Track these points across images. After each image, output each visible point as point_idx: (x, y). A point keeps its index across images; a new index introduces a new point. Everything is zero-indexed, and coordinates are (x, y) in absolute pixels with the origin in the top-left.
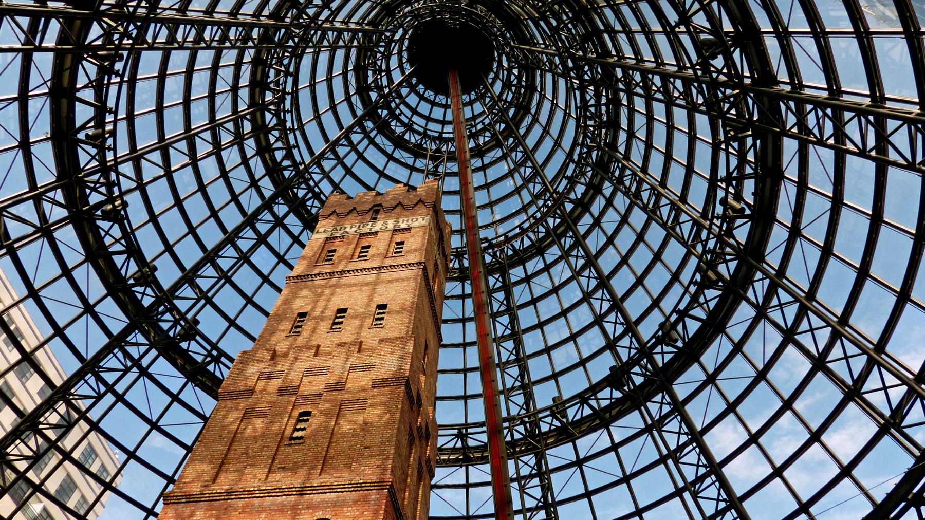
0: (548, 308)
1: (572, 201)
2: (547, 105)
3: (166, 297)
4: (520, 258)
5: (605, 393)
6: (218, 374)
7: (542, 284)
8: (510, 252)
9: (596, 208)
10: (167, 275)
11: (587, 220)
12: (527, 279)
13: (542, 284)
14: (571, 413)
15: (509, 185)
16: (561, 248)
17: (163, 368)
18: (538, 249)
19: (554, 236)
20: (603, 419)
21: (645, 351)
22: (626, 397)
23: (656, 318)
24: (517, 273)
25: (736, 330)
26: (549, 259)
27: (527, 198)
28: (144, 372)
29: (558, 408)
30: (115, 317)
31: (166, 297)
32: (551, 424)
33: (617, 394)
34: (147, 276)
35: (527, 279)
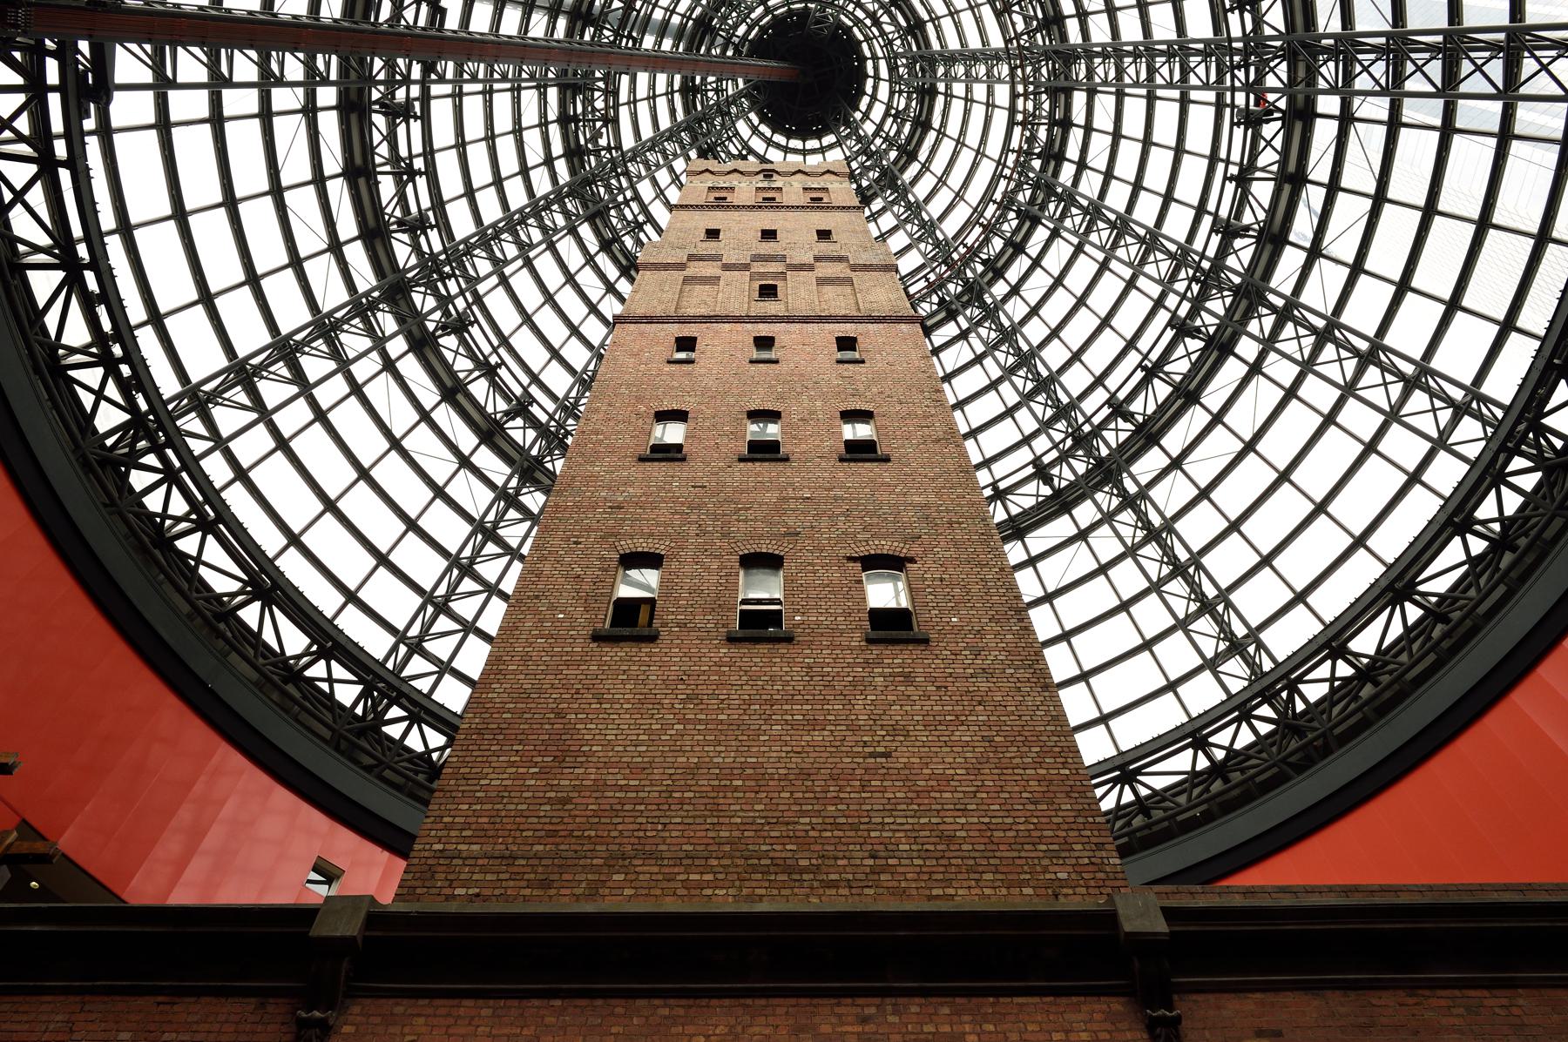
1: (1039, 156)
5: (1180, 351)
8: (980, 268)
9: (1073, 152)
11: (1068, 171)
12: (1015, 290)
13: (1038, 283)
14: (1136, 406)
20: (1187, 394)
21: (1210, 279)
22: (1210, 341)
23: (1207, 221)
24: (1000, 289)
25: (1320, 170)
30: (498, 470)
32: (1117, 430)
33: (1195, 345)
35: (1015, 290)
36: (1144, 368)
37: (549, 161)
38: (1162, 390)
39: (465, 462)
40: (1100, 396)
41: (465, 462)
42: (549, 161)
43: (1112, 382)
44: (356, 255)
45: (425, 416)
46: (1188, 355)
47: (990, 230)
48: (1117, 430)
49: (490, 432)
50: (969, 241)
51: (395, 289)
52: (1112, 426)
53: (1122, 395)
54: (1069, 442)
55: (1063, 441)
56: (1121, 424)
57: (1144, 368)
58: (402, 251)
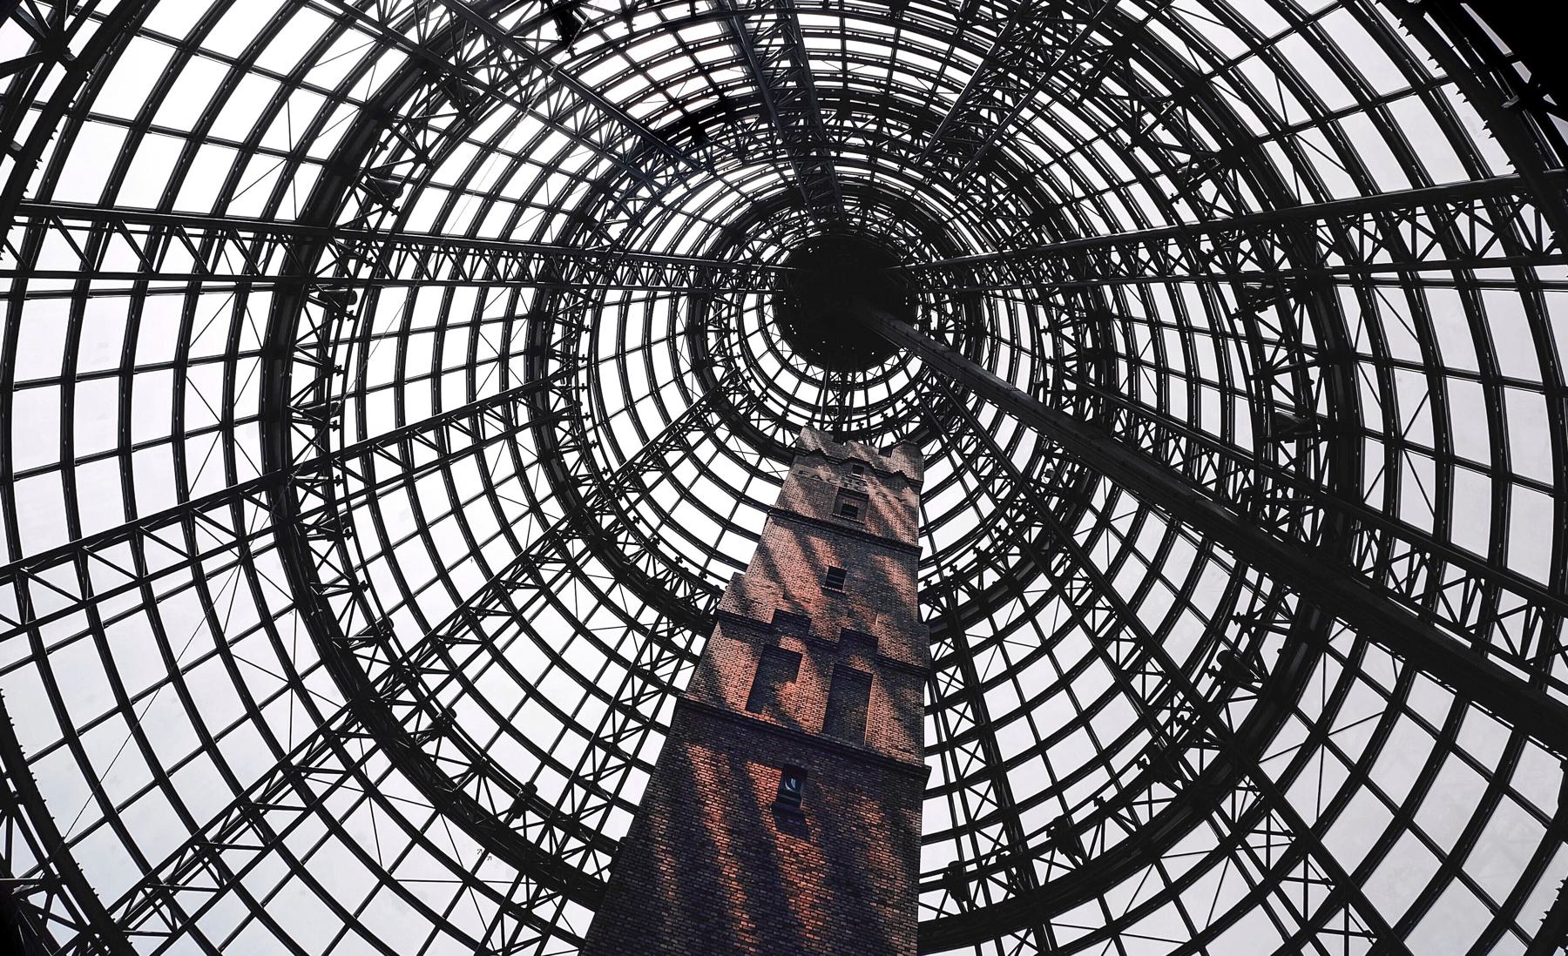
0: (1038, 677)
2: (1005, 351)
3: (405, 672)
4: (984, 604)
6: (484, 802)
7: (1023, 641)
10: (407, 633)
15: (955, 494)
16: (1050, 576)
17: (399, 787)
18: (1012, 586)
19: (1036, 559)
24: (979, 631)
26: (1032, 599)
27: (986, 505)
28: (371, 791)
29: (1064, 834)
31: (405, 672)
32: (1051, 863)
34: (380, 632)
35: (998, 638)
36: (1099, 802)
37: (503, 358)
38: (1115, 834)
39: (295, 682)
40: (1050, 810)
41: (295, 682)
42: (503, 358)
43: (1073, 795)
44: (249, 438)
45: (267, 622)
46: (1150, 802)
47: (984, 560)
48: (1051, 863)
49: (336, 654)
50: (960, 564)
51: (279, 477)
52: (1047, 856)
53: (1077, 818)
54: (993, 860)
55: (988, 857)
56: (1060, 858)
57: (1099, 802)
58: (301, 442)
